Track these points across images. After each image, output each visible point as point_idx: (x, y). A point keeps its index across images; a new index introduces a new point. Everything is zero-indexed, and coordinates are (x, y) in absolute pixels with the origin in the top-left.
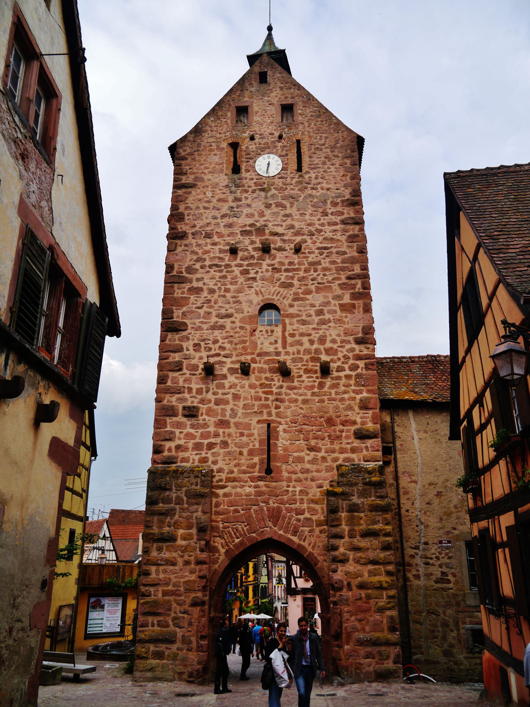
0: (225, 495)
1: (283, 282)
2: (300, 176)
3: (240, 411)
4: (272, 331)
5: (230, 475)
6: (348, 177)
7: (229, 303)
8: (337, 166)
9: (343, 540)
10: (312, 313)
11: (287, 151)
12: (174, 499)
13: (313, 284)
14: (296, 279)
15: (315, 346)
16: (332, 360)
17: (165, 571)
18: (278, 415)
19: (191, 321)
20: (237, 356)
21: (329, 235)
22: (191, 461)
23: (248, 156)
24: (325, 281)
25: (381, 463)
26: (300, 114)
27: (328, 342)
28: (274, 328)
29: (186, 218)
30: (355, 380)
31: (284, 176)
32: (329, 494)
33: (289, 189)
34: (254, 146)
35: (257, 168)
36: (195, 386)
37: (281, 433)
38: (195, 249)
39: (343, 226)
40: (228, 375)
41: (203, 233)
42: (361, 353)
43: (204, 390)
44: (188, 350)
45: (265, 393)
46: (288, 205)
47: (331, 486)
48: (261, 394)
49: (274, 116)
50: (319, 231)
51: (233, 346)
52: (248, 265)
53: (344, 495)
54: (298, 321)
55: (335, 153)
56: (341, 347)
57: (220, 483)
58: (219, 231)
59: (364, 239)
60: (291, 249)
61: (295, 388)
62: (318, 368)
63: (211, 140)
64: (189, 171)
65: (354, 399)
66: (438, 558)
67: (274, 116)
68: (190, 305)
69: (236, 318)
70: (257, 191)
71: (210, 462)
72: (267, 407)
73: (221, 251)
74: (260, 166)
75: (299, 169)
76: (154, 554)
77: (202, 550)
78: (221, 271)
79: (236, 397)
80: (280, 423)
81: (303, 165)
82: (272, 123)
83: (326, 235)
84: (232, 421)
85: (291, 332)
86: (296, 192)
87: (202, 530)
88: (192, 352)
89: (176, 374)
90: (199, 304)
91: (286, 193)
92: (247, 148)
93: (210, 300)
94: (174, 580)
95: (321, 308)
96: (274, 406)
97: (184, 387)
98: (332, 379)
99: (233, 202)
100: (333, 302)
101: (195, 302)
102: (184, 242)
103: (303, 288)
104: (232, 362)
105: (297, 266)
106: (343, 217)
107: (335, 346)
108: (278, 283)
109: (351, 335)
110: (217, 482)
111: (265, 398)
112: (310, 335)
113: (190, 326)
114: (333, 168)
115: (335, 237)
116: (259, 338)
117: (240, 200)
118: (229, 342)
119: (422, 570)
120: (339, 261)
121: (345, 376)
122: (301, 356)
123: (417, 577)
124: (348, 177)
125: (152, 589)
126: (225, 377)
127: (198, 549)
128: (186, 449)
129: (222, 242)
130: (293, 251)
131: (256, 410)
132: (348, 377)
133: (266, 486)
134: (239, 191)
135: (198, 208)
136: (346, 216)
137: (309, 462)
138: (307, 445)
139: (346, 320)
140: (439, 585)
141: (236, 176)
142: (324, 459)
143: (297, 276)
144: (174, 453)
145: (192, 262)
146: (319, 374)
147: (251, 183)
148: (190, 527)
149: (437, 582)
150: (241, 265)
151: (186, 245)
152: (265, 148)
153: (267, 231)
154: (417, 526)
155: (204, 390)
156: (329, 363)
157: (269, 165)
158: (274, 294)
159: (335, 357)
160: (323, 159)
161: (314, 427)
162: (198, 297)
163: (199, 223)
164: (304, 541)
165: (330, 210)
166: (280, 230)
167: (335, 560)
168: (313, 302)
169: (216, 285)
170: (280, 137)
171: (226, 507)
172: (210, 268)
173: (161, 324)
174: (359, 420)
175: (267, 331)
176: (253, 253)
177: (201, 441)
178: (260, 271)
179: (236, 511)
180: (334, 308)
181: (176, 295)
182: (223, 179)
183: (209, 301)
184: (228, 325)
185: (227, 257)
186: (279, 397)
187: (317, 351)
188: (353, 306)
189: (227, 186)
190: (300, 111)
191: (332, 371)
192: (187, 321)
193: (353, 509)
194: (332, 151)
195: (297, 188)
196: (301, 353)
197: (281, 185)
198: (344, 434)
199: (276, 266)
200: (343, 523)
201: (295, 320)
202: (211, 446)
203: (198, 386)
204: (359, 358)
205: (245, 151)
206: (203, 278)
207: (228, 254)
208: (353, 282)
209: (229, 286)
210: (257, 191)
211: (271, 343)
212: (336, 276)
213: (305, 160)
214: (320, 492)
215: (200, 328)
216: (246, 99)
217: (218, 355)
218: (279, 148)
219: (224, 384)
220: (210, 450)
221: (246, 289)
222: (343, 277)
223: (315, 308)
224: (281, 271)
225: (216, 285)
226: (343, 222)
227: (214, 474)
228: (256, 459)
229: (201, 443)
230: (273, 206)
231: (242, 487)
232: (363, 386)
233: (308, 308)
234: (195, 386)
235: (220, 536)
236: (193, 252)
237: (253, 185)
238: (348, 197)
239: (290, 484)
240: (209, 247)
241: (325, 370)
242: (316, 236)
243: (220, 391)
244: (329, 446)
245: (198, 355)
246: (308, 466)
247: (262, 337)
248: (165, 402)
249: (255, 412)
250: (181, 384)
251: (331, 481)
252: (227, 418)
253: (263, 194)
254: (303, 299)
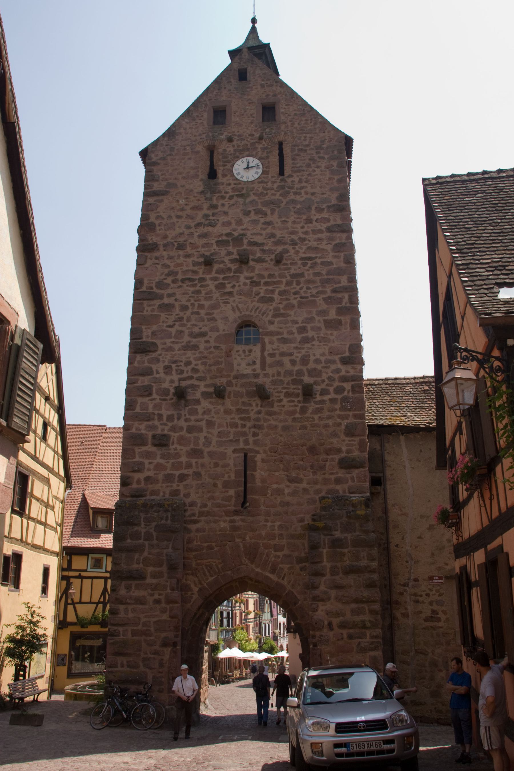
0: (198, 530)
1: (262, 297)
2: (282, 180)
3: (215, 440)
4: (250, 351)
5: (204, 509)
6: (335, 181)
7: (203, 321)
8: (323, 168)
9: (325, 578)
10: (295, 330)
11: (268, 153)
12: (143, 534)
13: (295, 298)
14: (277, 292)
15: (296, 368)
16: (315, 383)
17: (134, 610)
18: (255, 442)
19: (162, 341)
20: (211, 378)
21: (314, 244)
22: (162, 494)
23: (225, 160)
24: (309, 295)
25: (368, 494)
26: (282, 113)
27: (311, 362)
28: (251, 347)
29: (158, 228)
30: (341, 404)
31: (265, 180)
32: (312, 528)
33: (270, 194)
34: (232, 149)
35: (235, 172)
36: (165, 413)
37: (259, 464)
38: (167, 262)
39: (328, 234)
40: (202, 400)
41: (176, 244)
42: (349, 374)
43: (176, 417)
44: (158, 373)
45: (241, 419)
46: (269, 212)
47: (314, 520)
48: (237, 421)
49: (254, 115)
50: (303, 240)
51: (207, 367)
52: (224, 279)
53: (327, 529)
54: (278, 339)
55: (322, 155)
56: (326, 367)
57: (193, 518)
58: (192, 242)
59: (352, 248)
60: (271, 260)
61: (275, 413)
62: (300, 391)
64: (161, 177)
65: (340, 425)
66: (428, 595)
67: (254, 115)
68: (161, 324)
69: (210, 337)
70: (235, 198)
71: (182, 496)
72: (244, 434)
73: (195, 264)
74: (238, 169)
75: (282, 172)
76: (123, 592)
77: (172, 589)
78: (194, 285)
79: (210, 424)
80: (258, 452)
82: (252, 123)
83: (310, 244)
84: (206, 450)
85: (271, 351)
86: (278, 197)
87: (172, 568)
88: (162, 375)
89: (146, 400)
90: (170, 323)
91: (267, 198)
92: (225, 150)
93: (182, 318)
94: (144, 620)
95: (304, 324)
96: (251, 433)
97: (154, 414)
98: (316, 403)
99: (208, 209)
100: (317, 318)
101: (166, 320)
102: (156, 254)
103: (285, 303)
104: (206, 386)
105: (278, 279)
106: (329, 224)
107: (319, 367)
108: (257, 297)
109: (337, 354)
110: (190, 516)
111: (242, 424)
112: (291, 355)
113: (160, 347)
114: (318, 171)
115: (319, 246)
116: (235, 359)
117: (215, 207)
118: (202, 364)
119: (410, 608)
120: (324, 272)
121: (330, 399)
122: (282, 378)
123: (406, 615)
124: (335, 181)
125: (121, 629)
126: (198, 402)
127: (168, 588)
128: (157, 481)
129: (195, 253)
130: (273, 262)
131: (232, 437)
132: (333, 401)
133: (242, 520)
134: (215, 198)
135: (170, 217)
136: (332, 223)
137: (289, 494)
138: (287, 476)
139: (332, 338)
140: (429, 624)
141: (212, 182)
142: (305, 490)
143: (277, 291)
144: (142, 485)
145: (163, 277)
146: (301, 398)
147: (229, 189)
148: (161, 566)
149: (426, 620)
150: (216, 279)
151: (157, 258)
152: (243, 150)
153: (245, 242)
154: (407, 562)
155: (176, 417)
156: (311, 385)
158: (252, 310)
159: (319, 379)
160: (307, 161)
161: (295, 457)
162: (169, 315)
163: (171, 234)
164: (283, 579)
165: (315, 216)
166: (258, 239)
167: (315, 599)
168: (295, 318)
169: (189, 301)
170: (261, 138)
171: (199, 543)
172: (183, 282)
173: (130, 345)
174: (344, 449)
175: (244, 351)
176: (229, 265)
177: (172, 472)
178: (237, 284)
179: (210, 548)
180: (318, 325)
181: (145, 313)
182: (198, 185)
183: (181, 319)
184: (202, 347)
185: (201, 270)
186: (257, 423)
187: (300, 373)
188: (340, 322)
189: (202, 192)
190: (282, 110)
191: (316, 394)
192: (158, 342)
193: (336, 544)
194: (317, 153)
195: (279, 193)
196: (282, 374)
197: (261, 190)
198: (328, 464)
199: (255, 279)
200: (325, 560)
201: (275, 338)
202: (182, 478)
203: (169, 413)
204: (344, 379)
205: (222, 154)
206: (174, 294)
207: (203, 267)
208: (339, 295)
209: (203, 302)
210: (235, 198)
211: (248, 364)
212: (321, 289)
214: (301, 526)
215: (170, 349)
216: (224, 98)
217: (191, 378)
218: (259, 150)
219: (197, 409)
220: (182, 482)
221: (221, 304)
222: (328, 290)
223: (297, 325)
224: (260, 285)
225: (189, 301)
226: (329, 230)
227: (186, 508)
228: (232, 492)
229: (172, 474)
230: (253, 213)
231: (216, 522)
232: (349, 410)
233: (290, 325)
234: (165, 413)
235: (192, 574)
236: (166, 266)
237: (230, 191)
238: (334, 202)
239: (268, 518)
240: (182, 259)
241: (308, 393)
242: (299, 245)
243: (192, 418)
244: (311, 476)
245: (168, 378)
246: (288, 499)
247: (239, 358)
248: (134, 430)
249: (231, 441)
250: (150, 410)
251: (313, 515)
252: (201, 447)
253: (241, 200)
254: (283, 315)
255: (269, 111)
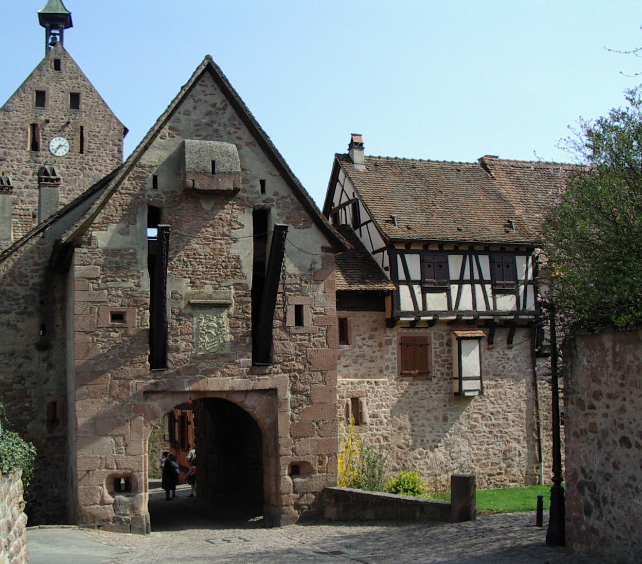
26: (84, 103)
35: (51, 148)
63: (16, 119)
75: (81, 152)
81: (84, 144)
157: (59, 146)
170: (68, 123)
213: (86, 144)
255: (75, 99)
